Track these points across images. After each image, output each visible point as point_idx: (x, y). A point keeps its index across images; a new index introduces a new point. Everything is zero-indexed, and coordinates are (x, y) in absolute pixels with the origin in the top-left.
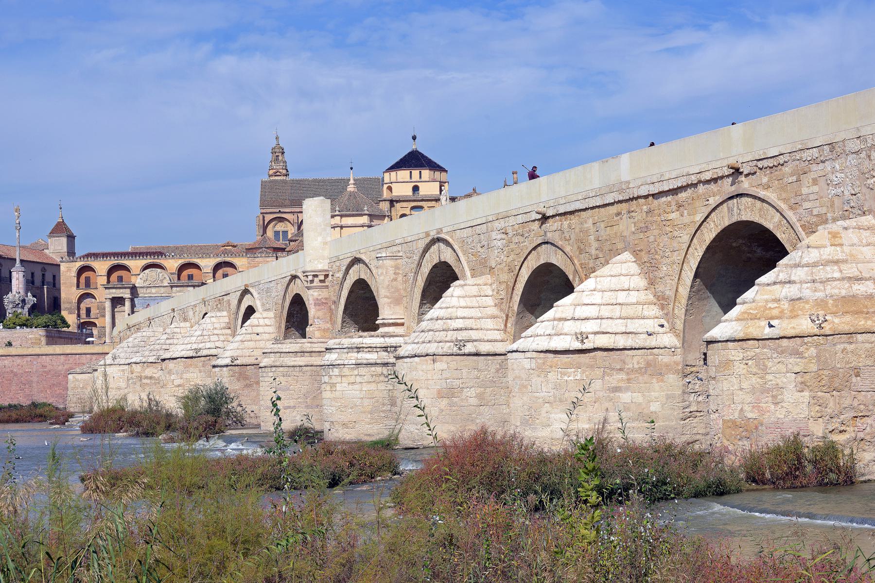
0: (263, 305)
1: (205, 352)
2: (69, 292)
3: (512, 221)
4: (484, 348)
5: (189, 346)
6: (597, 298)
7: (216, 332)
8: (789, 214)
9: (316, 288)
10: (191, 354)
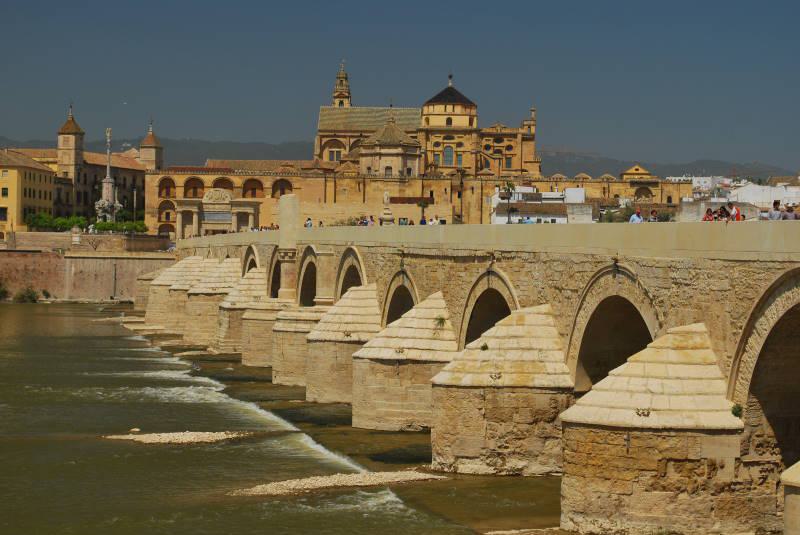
0: (261, 260)
1: (220, 291)
2: (152, 199)
3: (388, 250)
5: (209, 285)
6: (415, 323)
8: (514, 291)
9: (287, 262)
10: (210, 291)
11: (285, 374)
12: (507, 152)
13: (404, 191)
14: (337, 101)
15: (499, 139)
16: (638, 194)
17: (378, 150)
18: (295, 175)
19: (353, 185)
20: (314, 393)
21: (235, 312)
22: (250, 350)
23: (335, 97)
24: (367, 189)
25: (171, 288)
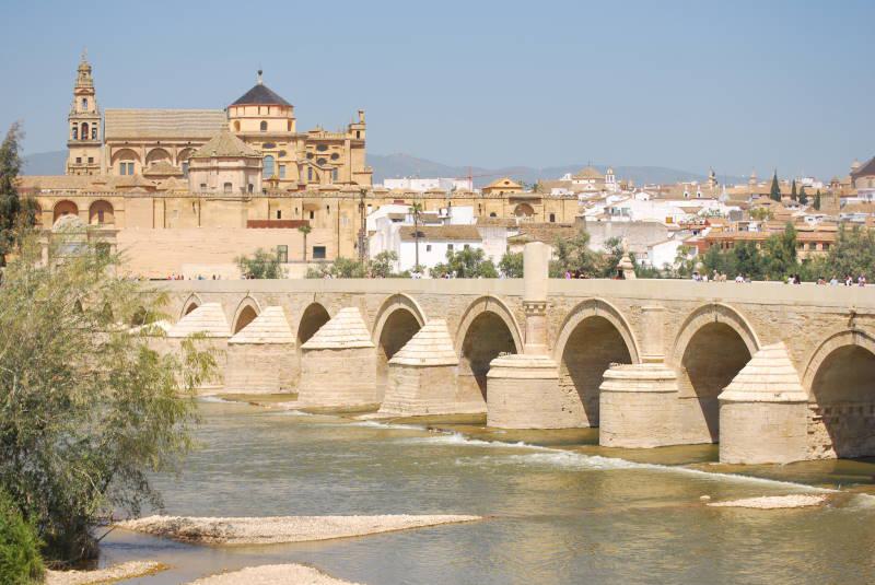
1: (349, 345)
3: (813, 309)
4: (794, 397)
5: (333, 339)
7: (355, 326)
9: (537, 315)
10: (338, 346)
11: (626, 436)
12: (333, 162)
13: (247, 211)
14: (80, 99)
15: (322, 146)
16: (518, 212)
17: (215, 163)
18: (116, 195)
19: (186, 205)
20: (741, 456)
21: (426, 369)
22: (505, 411)
23: (77, 95)
24: (203, 208)
25: (231, 341)
